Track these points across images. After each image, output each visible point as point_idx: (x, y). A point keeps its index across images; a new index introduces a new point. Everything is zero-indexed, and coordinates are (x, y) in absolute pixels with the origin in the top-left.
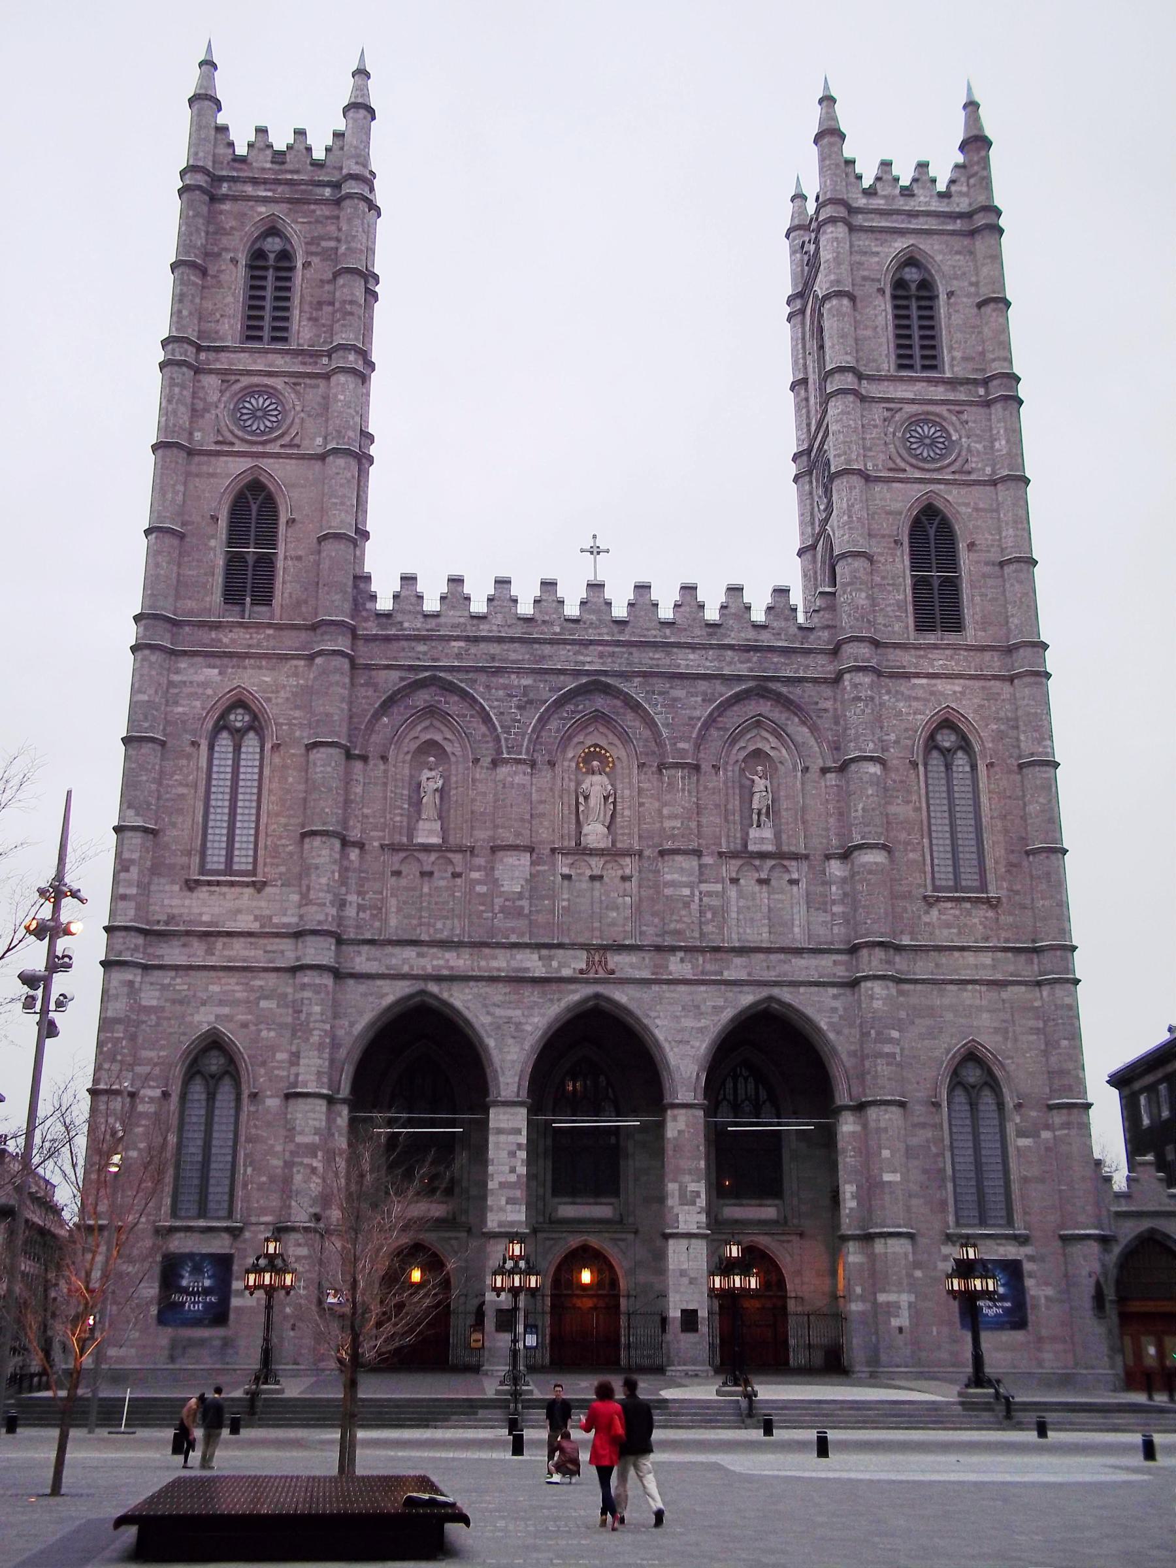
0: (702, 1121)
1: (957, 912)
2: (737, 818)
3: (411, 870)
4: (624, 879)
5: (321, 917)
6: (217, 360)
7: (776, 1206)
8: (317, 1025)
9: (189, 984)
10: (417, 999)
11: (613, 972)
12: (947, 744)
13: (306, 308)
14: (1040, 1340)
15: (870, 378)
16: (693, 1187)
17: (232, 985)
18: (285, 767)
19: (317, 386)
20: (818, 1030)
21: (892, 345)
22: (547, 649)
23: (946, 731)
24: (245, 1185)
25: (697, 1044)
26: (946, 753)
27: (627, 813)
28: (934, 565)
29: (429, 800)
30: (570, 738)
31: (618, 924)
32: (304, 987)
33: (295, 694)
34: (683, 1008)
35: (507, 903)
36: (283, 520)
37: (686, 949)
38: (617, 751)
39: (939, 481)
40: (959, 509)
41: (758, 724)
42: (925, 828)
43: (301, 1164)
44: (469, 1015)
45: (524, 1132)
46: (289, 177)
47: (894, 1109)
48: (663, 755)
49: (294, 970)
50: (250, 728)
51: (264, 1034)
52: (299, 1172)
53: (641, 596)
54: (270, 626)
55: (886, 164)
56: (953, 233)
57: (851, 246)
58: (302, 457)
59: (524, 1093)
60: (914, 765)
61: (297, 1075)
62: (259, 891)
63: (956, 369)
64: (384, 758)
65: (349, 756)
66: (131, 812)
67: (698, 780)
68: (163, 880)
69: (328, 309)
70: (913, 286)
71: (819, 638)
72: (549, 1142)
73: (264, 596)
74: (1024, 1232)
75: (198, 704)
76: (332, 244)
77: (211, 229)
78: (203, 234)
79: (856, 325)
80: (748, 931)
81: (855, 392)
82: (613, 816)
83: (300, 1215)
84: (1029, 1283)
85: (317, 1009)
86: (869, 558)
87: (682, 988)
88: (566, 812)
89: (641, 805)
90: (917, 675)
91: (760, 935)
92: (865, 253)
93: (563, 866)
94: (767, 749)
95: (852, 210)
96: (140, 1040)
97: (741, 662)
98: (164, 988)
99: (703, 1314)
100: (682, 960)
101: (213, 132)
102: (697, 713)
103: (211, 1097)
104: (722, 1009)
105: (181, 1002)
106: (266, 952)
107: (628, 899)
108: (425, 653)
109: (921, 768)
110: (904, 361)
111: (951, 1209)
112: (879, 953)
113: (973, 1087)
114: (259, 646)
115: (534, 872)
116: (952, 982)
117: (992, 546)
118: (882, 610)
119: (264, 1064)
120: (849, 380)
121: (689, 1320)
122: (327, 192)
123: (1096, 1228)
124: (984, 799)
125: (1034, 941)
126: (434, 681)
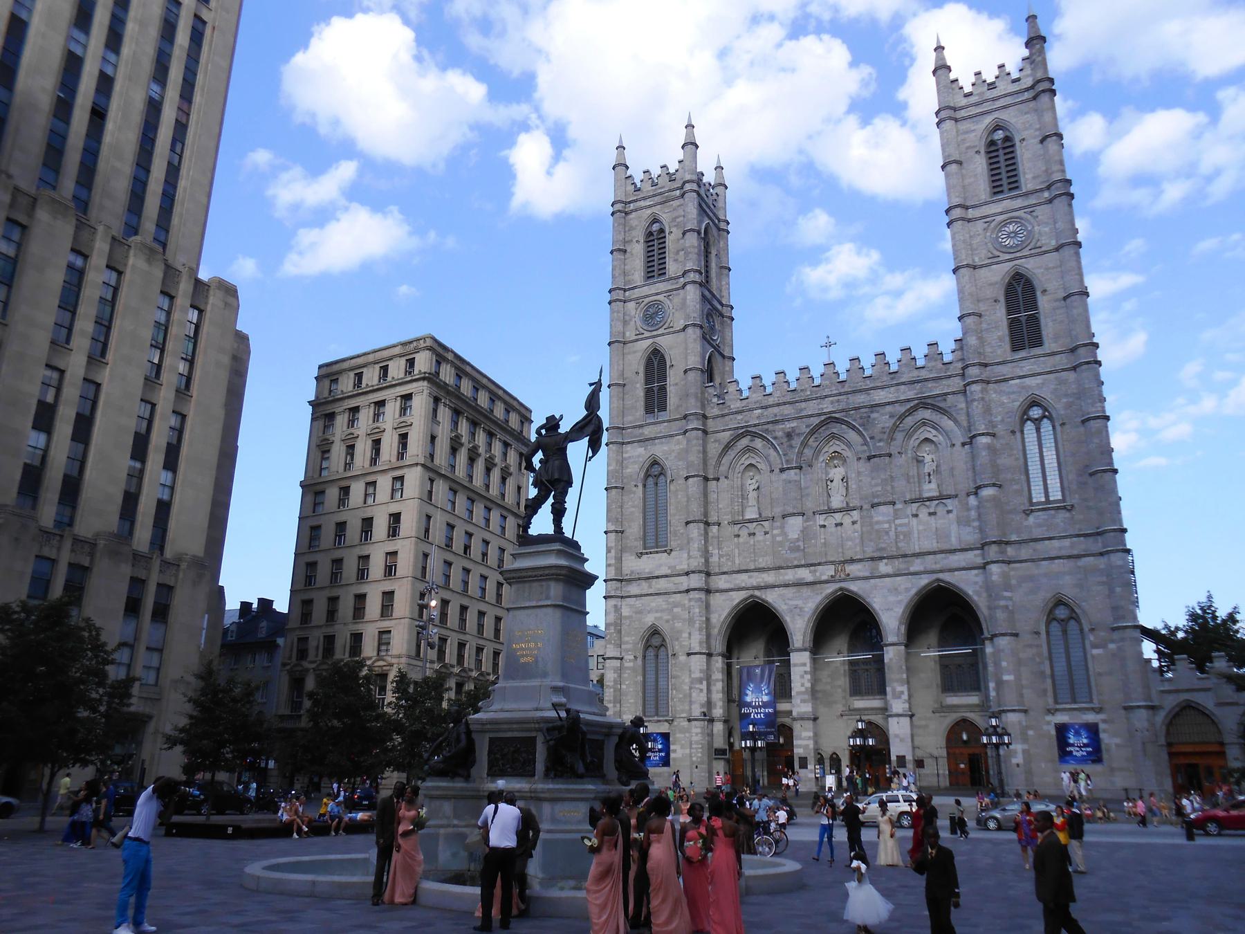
1: (1046, 517)
2: (916, 480)
3: (744, 532)
4: (854, 523)
5: (696, 564)
6: (634, 294)
11: (848, 575)
12: (1036, 417)
13: (671, 255)
14: (1112, 770)
15: (974, 207)
16: (899, 689)
17: (660, 599)
18: (677, 490)
19: (679, 294)
20: (967, 595)
21: (987, 183)
22: (803, 405)
23: (1035, 408)
24: (672, 699)
25: (896, 610)
26: (1037, 422)
27: (854, 486)
28: (1022, 309)
29: (752, 495)
30: (820, 451)
31: (853, 550)
32: (690, 600)
33: (679, 453)
34: (889, 590)
36: (668, 367)
37: (887, 558)
38: (847, 453)
39: (1021, 258)
40: (1035, 271)
41: (924, 424)
42: (1023, 470)
43: (695, 688)
44: (776, 605)
45: (808, 665)
46: (660, 191)
47: (1008, 638)
48: (870, 450)
49: (687, 591)
50: (661, 474)
51: (676, 625)
53: (853, 364)
54: (664, 422)
55: (978, 74)
56: (1022, 102)
57: (957, 132)
58: (674, 332)
59: (809, 644)
60: (1013, 432)
62: (669, 554)
63: (1029, 186)
64: (726, 477)
65: (706, 479)
66: (610, 524)
67: (891, 463)
68: (627, 554)
69: (682, 253)
70: (999, 142)
71: (956, 367)
72: (847, 667)
73: (663, 408)
74: (1097, 706)
75: (636, 466)
76: (682, 219)
77: (627, 229)
78: (623, 233)
79: (963, 177)
80: (926, 543)
81: (963, 219)
82: (847, 489)
83: (697, 711)
84: (1102, 736)
85: (697, 610)
86: (980, 316)
87: (887, 579)
88: (821, 490)
89: (861, 481)
90: (1012, 379)
91: (929, 544)
92: (967, 132)
93: (820, 520)
94: (930, 437)
95: (955, 109)
96: (623, 633)
97: (909, 390)
98: (631, 606)
100: (886, 564)
101: (624, 181)
102: (887, 425)
104: (912, 588)
108: (742, 420)
109: (1018, 435)
110: (997, 189)
111: (1050, 693)
112: (994, 548)
113: (1062, 620)
114: (661, 432)
115: (805, 525)
116: (1044, 559)
117: (1058, 289)
118: (989, 343)
119: (677, 639)
120: (957, 213)
121: (901, 760)
122: (678, 193)
123: (1145, 701)
124: (1060, 446)
125: (1098, 528)
126: (747, 432)
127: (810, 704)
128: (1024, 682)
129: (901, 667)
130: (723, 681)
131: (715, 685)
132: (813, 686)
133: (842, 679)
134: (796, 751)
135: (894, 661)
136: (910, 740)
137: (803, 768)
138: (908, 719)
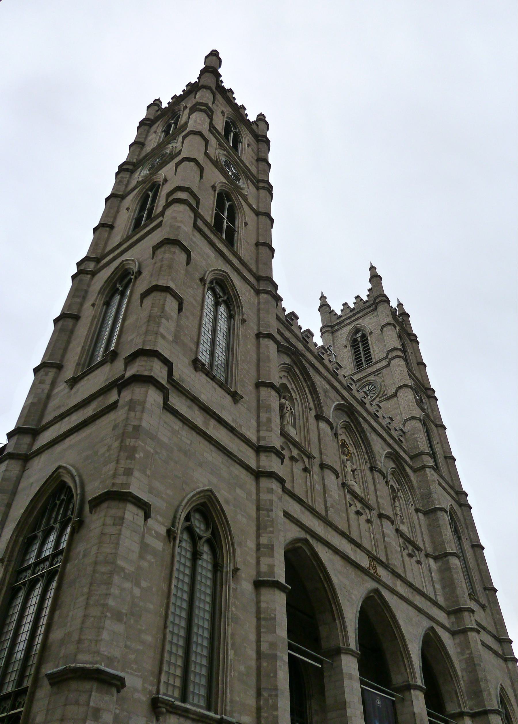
9: (192, 442)
10: (299, 545)
32: (270, 491)
35: (334, 504)
61: (271, 567)
75: (204, 262)
103: (196, 556)
105: (186, 453)
106: (239, 450)
107: (372, 534)
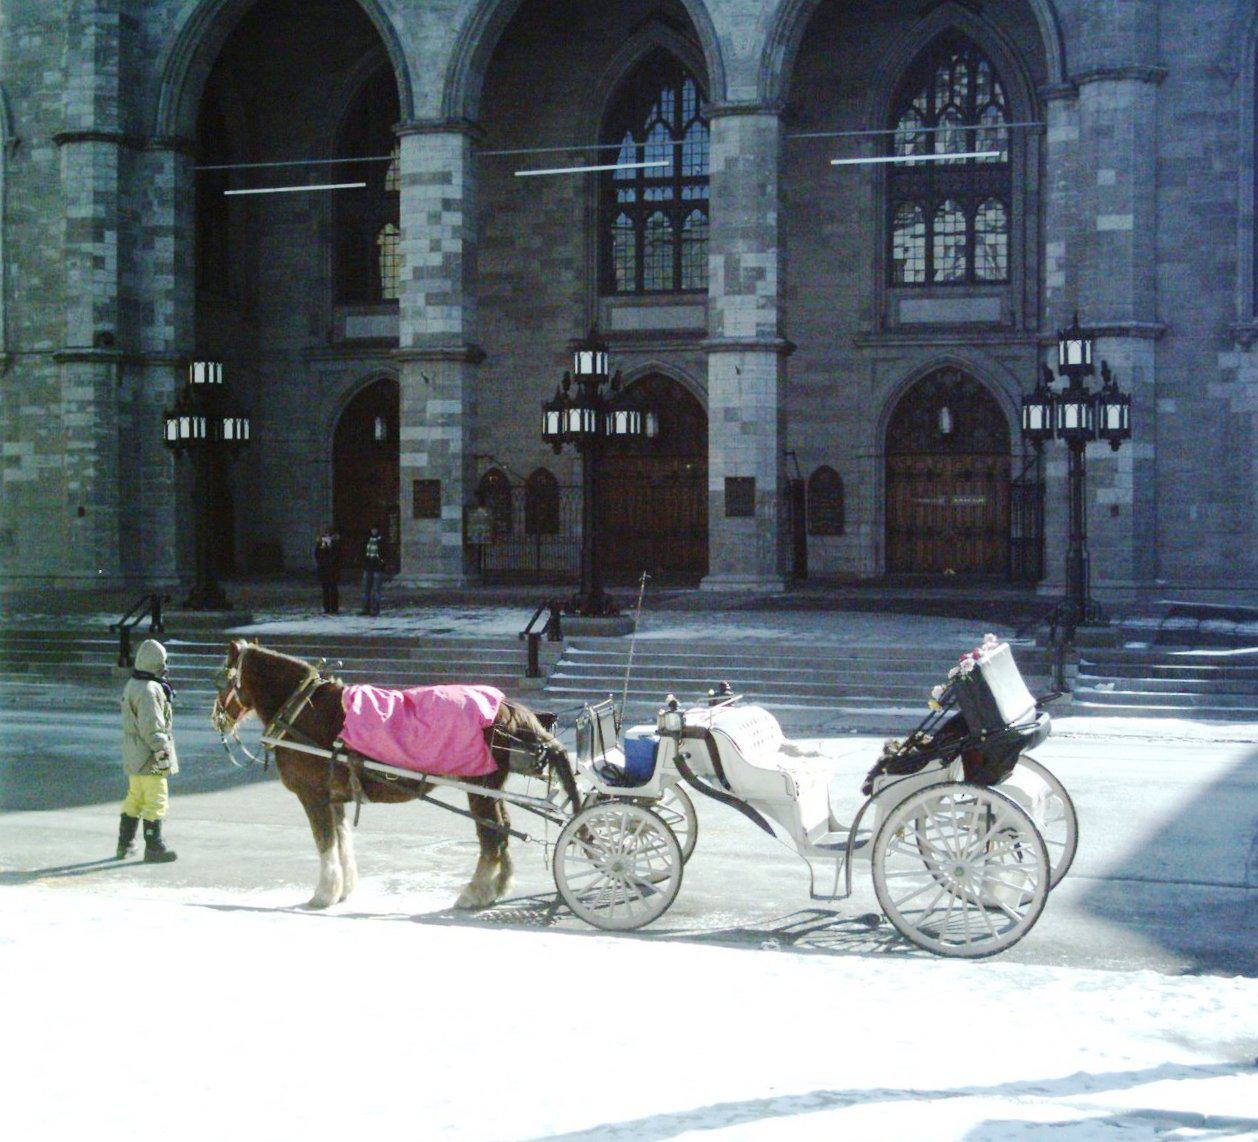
0: (773, 137)
7: (998, 295)
8: (91, 17)
16: (750, 260)
45: (457, 179)
52: (74, 265)
83: (81, 331)
99: (767, 483)
119: (25, 93)
121: (740, 491)
127: (457, 312)
128: (1166, 241)
129: (762, 186)
130: (178, 233)
131: (149, 245)
132: (469, 252)
133: (578, 238)
134: (407, 460)
135: (741, 166)
136: (772, 428)
137: (426, 516)
138: (773, 358)
